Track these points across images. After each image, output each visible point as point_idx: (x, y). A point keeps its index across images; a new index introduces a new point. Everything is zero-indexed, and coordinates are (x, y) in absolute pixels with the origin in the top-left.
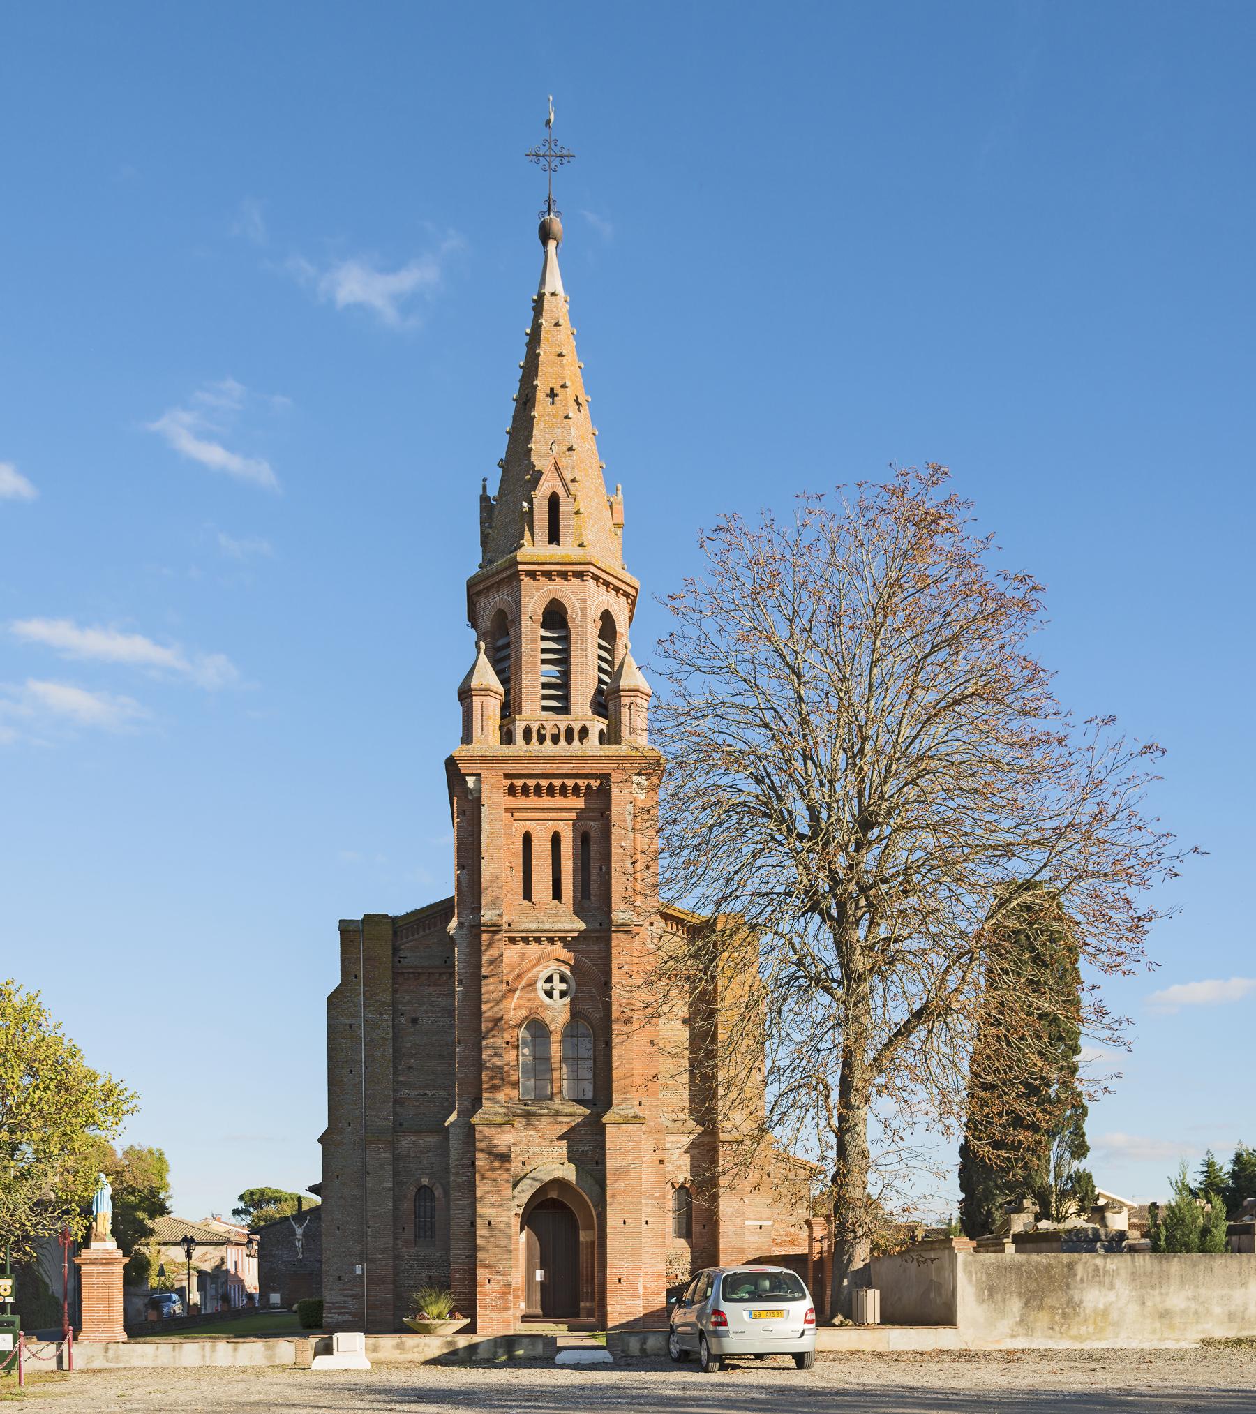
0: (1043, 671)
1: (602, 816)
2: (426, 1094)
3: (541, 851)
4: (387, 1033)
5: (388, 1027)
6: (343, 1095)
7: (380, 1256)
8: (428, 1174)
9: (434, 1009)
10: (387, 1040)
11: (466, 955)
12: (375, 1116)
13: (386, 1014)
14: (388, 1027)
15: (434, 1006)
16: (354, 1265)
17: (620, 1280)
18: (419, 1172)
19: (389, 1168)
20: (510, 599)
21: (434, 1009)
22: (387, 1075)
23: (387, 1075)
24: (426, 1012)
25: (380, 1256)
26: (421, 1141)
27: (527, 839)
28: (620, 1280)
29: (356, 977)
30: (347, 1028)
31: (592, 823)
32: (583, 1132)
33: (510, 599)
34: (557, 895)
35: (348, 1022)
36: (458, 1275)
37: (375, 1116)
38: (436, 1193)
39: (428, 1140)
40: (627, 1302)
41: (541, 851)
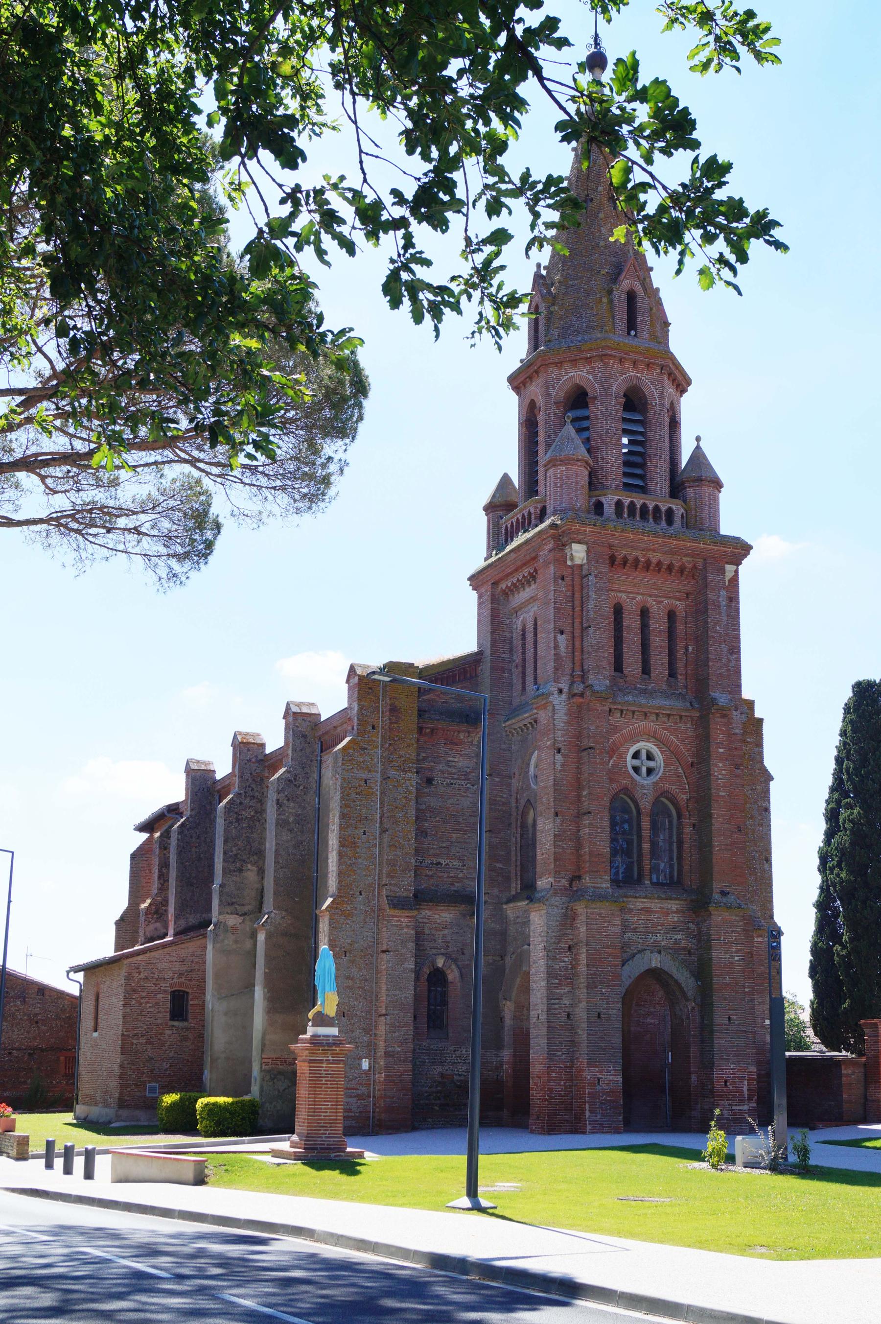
0: (345, 450)
1: (687, 597)
2: (439, 863)
3: (632, 622)
4: (410, 792)
5: (412, 786)
6: (356, 858)
7: (399, 1049)
8: (442, 954)
9: (450, 770)
10: (410, 800)
11: (565, 723)
12: (395, 885)
13: (410, 771)
14: (412, 786)
15: (450, 767)
16: (360, 1058)
17: (726, 1082)
18: (434, 951)
19: (411, 945)
20: (591, 377)
21: (450, 770)
22: (409, 840)
23: (409, 840)
24: (442, 772)
25: (399, 1049)
26: (437, 916)
27: (618, 611)
28: (726, 1082)
29: (373, 728)
30: (363, 783)
31: (678, 603)
32: (676, 919)
33: (591, 377)
34: (646, 670)
35: (364, 776)
36: (554, 1075)
37: (395, 885)
38: (450, 977)
39: (443, 915)
40: (734, 1108)
41: (632, 622)
